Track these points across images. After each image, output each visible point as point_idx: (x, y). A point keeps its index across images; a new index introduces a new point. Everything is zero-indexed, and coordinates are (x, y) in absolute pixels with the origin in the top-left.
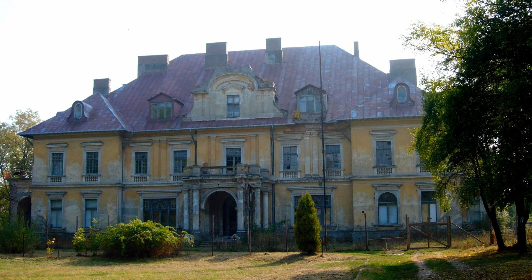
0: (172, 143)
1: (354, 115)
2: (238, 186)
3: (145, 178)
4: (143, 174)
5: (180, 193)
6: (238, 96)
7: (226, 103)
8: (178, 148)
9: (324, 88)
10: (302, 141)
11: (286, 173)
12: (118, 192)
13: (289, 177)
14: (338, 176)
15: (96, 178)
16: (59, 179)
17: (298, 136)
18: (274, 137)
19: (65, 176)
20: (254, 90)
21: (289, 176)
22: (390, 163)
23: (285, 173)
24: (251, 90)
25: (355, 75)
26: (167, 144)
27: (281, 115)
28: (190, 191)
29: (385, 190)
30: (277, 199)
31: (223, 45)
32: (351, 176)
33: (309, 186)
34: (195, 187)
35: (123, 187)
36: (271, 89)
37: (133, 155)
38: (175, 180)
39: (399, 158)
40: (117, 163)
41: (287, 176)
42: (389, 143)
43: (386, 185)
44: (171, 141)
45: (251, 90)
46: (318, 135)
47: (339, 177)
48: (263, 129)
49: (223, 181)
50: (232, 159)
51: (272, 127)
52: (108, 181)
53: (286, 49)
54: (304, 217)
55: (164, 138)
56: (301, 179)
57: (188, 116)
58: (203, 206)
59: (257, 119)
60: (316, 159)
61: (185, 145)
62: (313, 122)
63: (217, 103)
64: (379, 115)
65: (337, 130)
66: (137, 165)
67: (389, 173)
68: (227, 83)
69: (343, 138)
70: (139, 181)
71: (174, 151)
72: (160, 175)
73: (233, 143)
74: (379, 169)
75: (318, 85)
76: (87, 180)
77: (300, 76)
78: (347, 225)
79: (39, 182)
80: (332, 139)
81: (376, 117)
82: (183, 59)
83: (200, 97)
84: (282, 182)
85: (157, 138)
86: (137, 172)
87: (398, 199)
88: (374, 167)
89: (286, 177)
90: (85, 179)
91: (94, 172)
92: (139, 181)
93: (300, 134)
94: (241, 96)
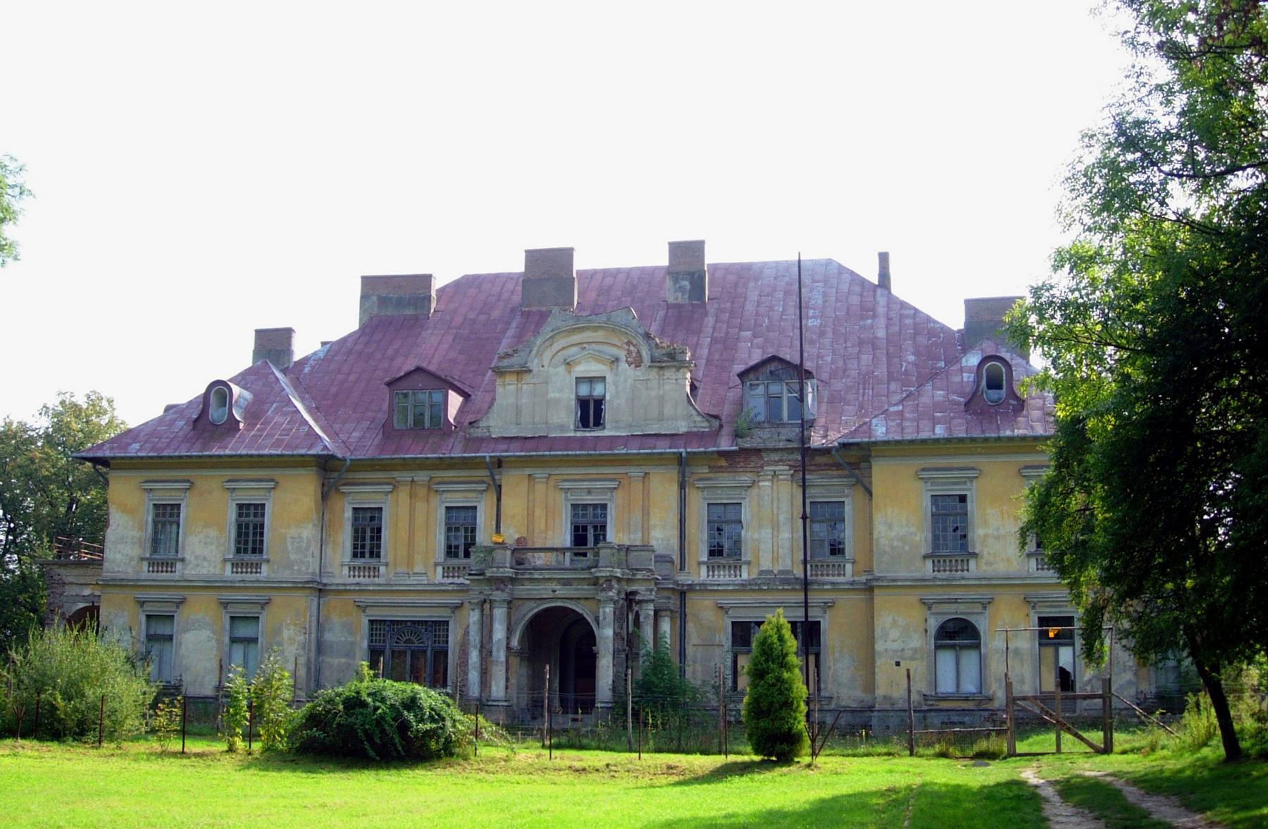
0: (443, 488)
1: (880, 431)
2: (601, 596)
5: (457, 607)
6: (603, 379)
7: (573, 397)
8: (458, 500)
9: (808, 365)
10: (754, 491)
13: (723, 577)
14: (839, 575)
15: (258, 566)
16: (169, 565)
17: (745, 478)
18: (687, 479)
19: (183, 560)
20: (640, 366)
21: (722, 573)
22: (964, 547)
23: (711, 568)
25: (881, 334)
26: (429, 489)
27: (703, 426)
28: (485, 604)
29: (952, 611)
30: (690, 627)
31: (566, 255)
32: (869, 577)
34: (498, 595)
35: (321, 590)
36: (681, 365)
37: (349, 514)
39: (986, 535)
40: (309, 532)
41: (716, 573)
42: (963, 499)
43: (956, 601)
44: (438, 484)
45: (633, 366)
46: (792, 476)
48: (659, 459)
49: (567, 582)
50: (585, 528)
51: (684, 455)
52: (286, 575)
53: (715, 267)
54: (770, 678)
55: (422, 476)
56: (751, 582)
57: (482, 424)
58: (515, 643)
60: (785, 535)
61: (474, 495)
62: (781, 445)
63: (552, 395)
64: (940, 431)
65: (838, 466)
66: (355, 538)
67: (962, 571)
68: (574, 350)
69: (853, 485)
70: (359, 576)
71: (447, 508)
72: (410, 563)
73: (589, 492)
74: (939, 561)
75: (791, 355)
76: (235, 570)
77: (748, 334)
78: (858, 694)
79: (119, 572)
80: (825, 487)
81: (932, 437)
83: (510, 379)
84: (704, 588)
85: (406, 476)
86: (355, 555)
87: (982, 634)
88: (925, 557)
89: (713, 576)
91: (254, 551)
92: (359, 576)
93: (748, 475)
94: (609, 378)
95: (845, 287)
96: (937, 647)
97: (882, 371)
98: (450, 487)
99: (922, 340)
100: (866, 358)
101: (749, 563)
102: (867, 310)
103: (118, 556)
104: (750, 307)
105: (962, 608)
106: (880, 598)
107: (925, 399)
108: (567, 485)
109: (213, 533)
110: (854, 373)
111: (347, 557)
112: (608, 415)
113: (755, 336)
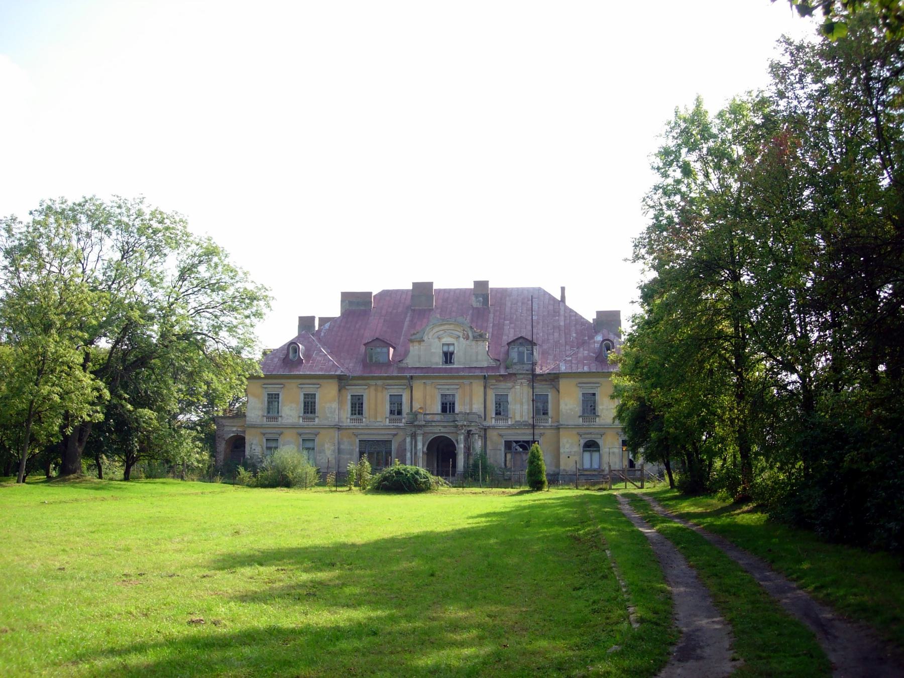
1: (563, 368)
5: (395, 435)
6: (453, 344)
8: (395, 392)
9: (535, 341)
12: (335, 434)
13: (501, 423)
15: (314, 419)
16: (276, 418)
17: (509, 385)
19: (281, 416)
22: (595, 413)
23: (496, 420)
25: (562, 323)
26: (383, 388)
27: (493, 364)
28: (414, 436)
30: (488, 443)
31: (431, 284)
33: (519, 431)
34: (419, 432)
35: (339, 428)
36: (485, 340)
37: (349, 397)
39: (603, 409)
40: (335, 405)
42: (594, 394)
47: (547, 424)
48: (477, 377)
49: (445, 427)
50: (446, 404)
52: (326, 422)
53: (492, 289)
54: (535, 464)
55: (380, 382)
57: (404, 362)
58: (425, 449)
60: (525, 407)
62: (524, 372)
63: (433, 350)
64: (586, 369)
65: (546, 380)
66: (352, 407)
68: (442, 332)
72: (376, 418)
73: (448, 389)
75: (530, 338)
77: (508, 322)
78: (553, 468)
80: (541, 388)
82: (385, 294)
83: (416, 344)
84: (494, 428)
85: (372, 382)
86: (352, 414)
88: (580, 417)
91: (311, 413)
94: (456, 345)
95: (547, 301)
96: (584, 451)
97: (562, 341)
98: (392, 387)
99: (578, 327)
100: (556, 335)
101: (511, 418)
102: (556, 312)
103: (253, 415)
104: (508, 310)
105: (593, 436)
106: (562, 432)
107: (580, 355)
108: (439, 387)
109: (294, 405)
110: (551, 341)
111: (349, 415)
112: (455, 358)
113: (511, 323)
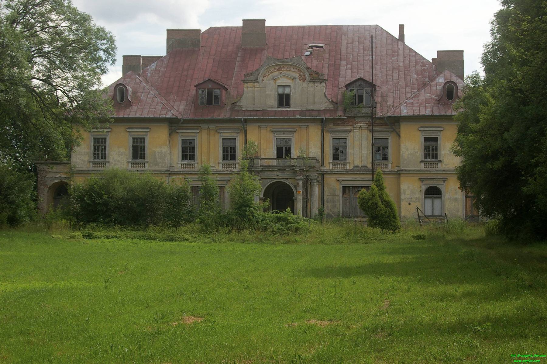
0: (221, 131)
2: (298, 177)
3: (193, 165)
4: (190, 161)
5: (228, 181)
7: (277, 93)
8: (228, 136)
10: (352, 134)
11: (335, 164)
13: (339, 168)
14: (386, 168)
15: (143, 164)
17: (348, 128)
18: (325, 128)
19: (109, 162)
20: (305, 81)
21: (339, 166)
23: (334, 164)
24: (302, 81)
25: (401, 64)
27: (331, 106)
29: (431, 183)
30: (326, 188)
32: (399, 169)
33: (358, 177)
38: (224, 168)
39: (445, 154)
40: (165, 149)
41: (336, 166)
43: (433, 179)
44: (220, 129)
45: (302, 81)
46: (367, 128)
47: (386, 170)
48: (314, 121)
51: (324, 119)
56: (351, 170)
59: (308, 110)
60: (364, 152)
61: (235, 134)
63: (267, 92)
64: (428, 112)
65: (386, 124)
67: (436, 167)
69: (392, 132)
70: (186, 168)
71: (223, 139)
73: (284, 133)
74: (426, 163)
75: (368, 78)
76: (133, 166)
79: (79, 167)
80: (381, 132)
81: (426, 115)
82: (212, 31)
83: (250, 85)
84: (331, 173)
85: (205, 126)
87: (443, 192)
88: (421, 162)
89: (335, 168)
90: (131, 165)
92: (186, 168)
93: (349, 127)
95: (384, 40)
96: (425, 197)
97: (402, 83)
98: (225, 131)
99: (419, 68)
100: (396, 76)
101: (349, 163)
102: (395, 53)
103: (78, 161)
104: (344, 49)
105: (435, 182)
106: (403, 178)
107: (422, 98)
108: (275, 130)
109: (122, 150)
110: (391, 83)
112: (291, 102)
113: (347, 64)
